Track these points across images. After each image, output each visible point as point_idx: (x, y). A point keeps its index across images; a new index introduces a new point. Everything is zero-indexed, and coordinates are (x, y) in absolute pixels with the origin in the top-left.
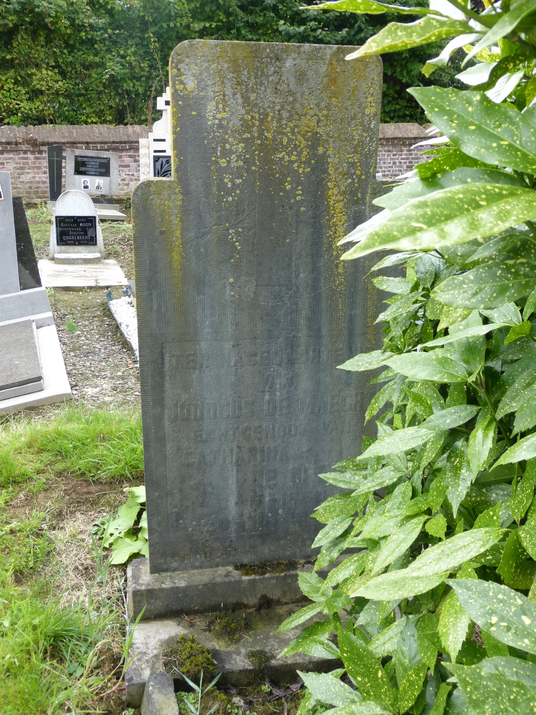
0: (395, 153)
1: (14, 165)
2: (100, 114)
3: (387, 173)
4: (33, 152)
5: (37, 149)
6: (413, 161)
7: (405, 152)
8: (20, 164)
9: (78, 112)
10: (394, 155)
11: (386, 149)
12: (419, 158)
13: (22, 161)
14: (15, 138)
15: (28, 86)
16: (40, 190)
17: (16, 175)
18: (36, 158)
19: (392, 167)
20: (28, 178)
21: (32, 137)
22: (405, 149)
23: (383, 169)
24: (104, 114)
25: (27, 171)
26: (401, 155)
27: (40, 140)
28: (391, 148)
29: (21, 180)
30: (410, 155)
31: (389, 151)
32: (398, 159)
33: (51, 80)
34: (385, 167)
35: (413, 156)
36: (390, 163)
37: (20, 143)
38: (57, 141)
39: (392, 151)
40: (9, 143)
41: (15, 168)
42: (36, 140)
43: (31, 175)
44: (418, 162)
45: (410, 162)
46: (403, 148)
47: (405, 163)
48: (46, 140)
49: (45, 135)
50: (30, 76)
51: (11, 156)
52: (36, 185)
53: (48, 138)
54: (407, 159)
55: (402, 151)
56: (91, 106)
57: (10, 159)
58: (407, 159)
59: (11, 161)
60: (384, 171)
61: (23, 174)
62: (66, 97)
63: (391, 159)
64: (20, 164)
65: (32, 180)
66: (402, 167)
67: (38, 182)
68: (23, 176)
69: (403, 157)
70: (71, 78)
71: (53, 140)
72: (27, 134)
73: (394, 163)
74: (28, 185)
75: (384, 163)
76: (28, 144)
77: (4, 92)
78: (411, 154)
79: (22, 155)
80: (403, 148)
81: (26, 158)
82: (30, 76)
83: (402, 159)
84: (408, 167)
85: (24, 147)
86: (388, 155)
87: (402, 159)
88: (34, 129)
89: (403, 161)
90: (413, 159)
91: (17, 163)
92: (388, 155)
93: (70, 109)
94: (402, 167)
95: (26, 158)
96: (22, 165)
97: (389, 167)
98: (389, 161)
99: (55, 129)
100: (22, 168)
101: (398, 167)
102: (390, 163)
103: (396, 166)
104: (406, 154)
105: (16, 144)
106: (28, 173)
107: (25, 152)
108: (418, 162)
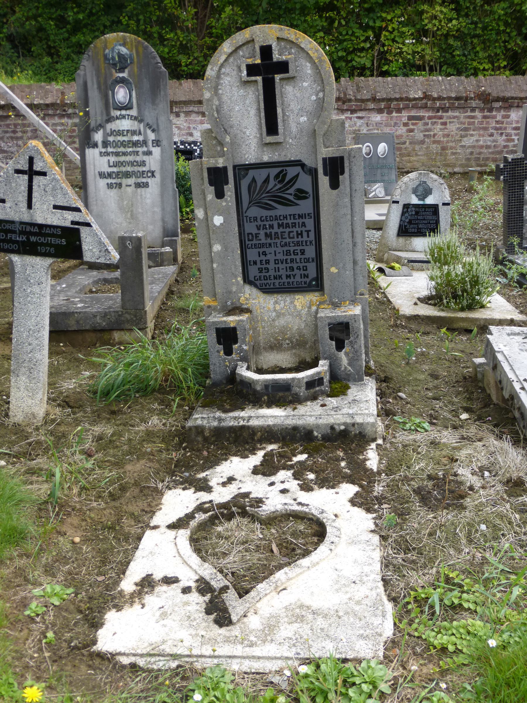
1: (458, 126)
2: (491, 60)
4: (482, 110)
5: (489, 106)
8: (464, 124)
9: (469, 57)
13: (468, 120)
14: (466, 92)
15: (414, 26)
16: (482, 156)
17: (457, 138)
18: (485, 117)
20: (471, 141)
21: (484, 91)
24: (498, 60)
25: (472, 132)
27: (495, 94)
29: (463, 144)
33: (444, 18)
37: (471, 99)
38: (514, 95)
40: (457, 99)
41: (458, 129)
42: (489, 94)
43: (474, 138)
48: (501, 95)
49: (499, 88)
50: (422, 12)
51: (457, 114)
52: (478, 150)
53: (502, 91)
56: (484, 49)
57: (454, 117)
59: (455, 120)
61: (466, 136)
62: (455, 37)
64: (464, 124)
65: (475, 144)
67: (482, 147)
68: (465, 139)
70: (467, 15)
71: (509, 95)
72: (479, 87)
74: (470, 150)
76: (480, 100)
77: (387, 34)
79: (469, 114)
81: (473, 117)
82: (422, 12)
85: (474, 104)
88: (486, 80)
91: (462, 123)
93: (461, 53)
95: (473, 117)
96: (466, 126)
99: (510, 81)
100: (466, 129)
105: (466, 99)
106: (472, 135)
107: (473, 110)
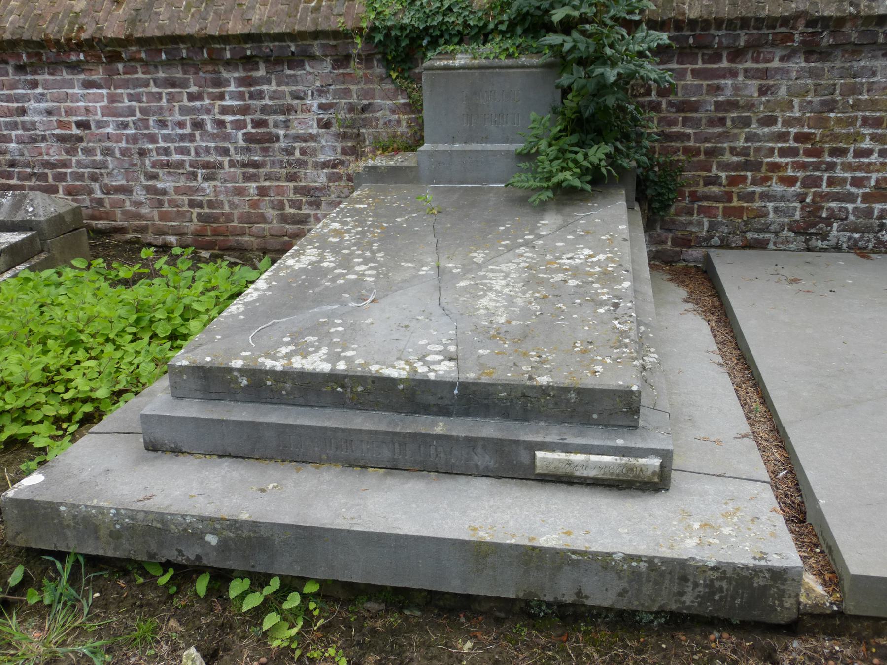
0: (194, 89)
3: (176, 157)
6: (271, 119)
7: (232, 88)
10: (192, 97)
11: (161, 75)
12: (289, 110)
19: (191, 138)
22: (232, 76)
23: (162, 144)
26: (221, 97)
28: (178, 74)
30: (252, 97)
31: (172, 83)
32: (208, 111)
34: (166, 138)
35: (267, 102)
36: (181, 125)
39: (184, 84)
44: (286, 124)
45: (257, 124)
46: (225, 75)
47: (239, 125)
54: (245, 110)
55: (219, 83)
58: (245, 110)
60: (166, 152)
63: (183, 111)
66: (226, 137)
69: (228, 103)
73: (198, 125)
75: (163, 124)
78: (260, 95)
80: (225, 75)
83: (224, 111)
84: (248, 138)
86: (171, 98)
87: (224, 111)
89: (228, 118)
90: (264, 110)
92: (171, 98)
94: (226, 137)
97: (182, 138)
98: (178, 117)
101: (214, 137)
102: (181, 125)
103: (205, 134)
104: (241, 96)
108: (286, 124)
